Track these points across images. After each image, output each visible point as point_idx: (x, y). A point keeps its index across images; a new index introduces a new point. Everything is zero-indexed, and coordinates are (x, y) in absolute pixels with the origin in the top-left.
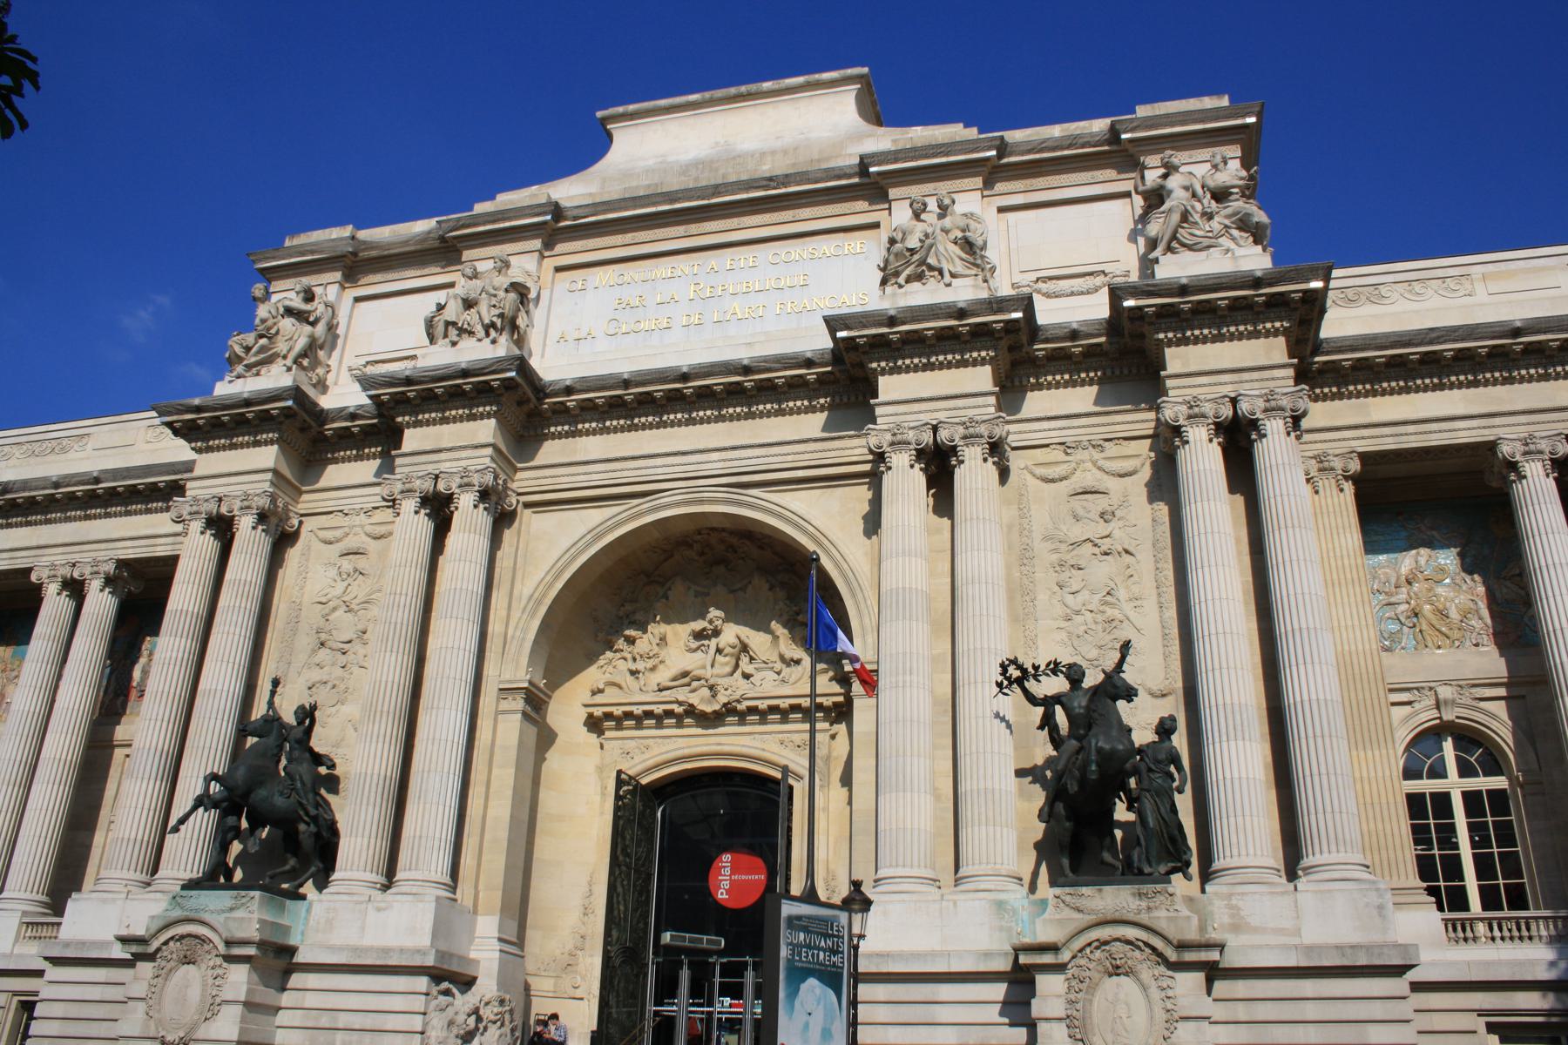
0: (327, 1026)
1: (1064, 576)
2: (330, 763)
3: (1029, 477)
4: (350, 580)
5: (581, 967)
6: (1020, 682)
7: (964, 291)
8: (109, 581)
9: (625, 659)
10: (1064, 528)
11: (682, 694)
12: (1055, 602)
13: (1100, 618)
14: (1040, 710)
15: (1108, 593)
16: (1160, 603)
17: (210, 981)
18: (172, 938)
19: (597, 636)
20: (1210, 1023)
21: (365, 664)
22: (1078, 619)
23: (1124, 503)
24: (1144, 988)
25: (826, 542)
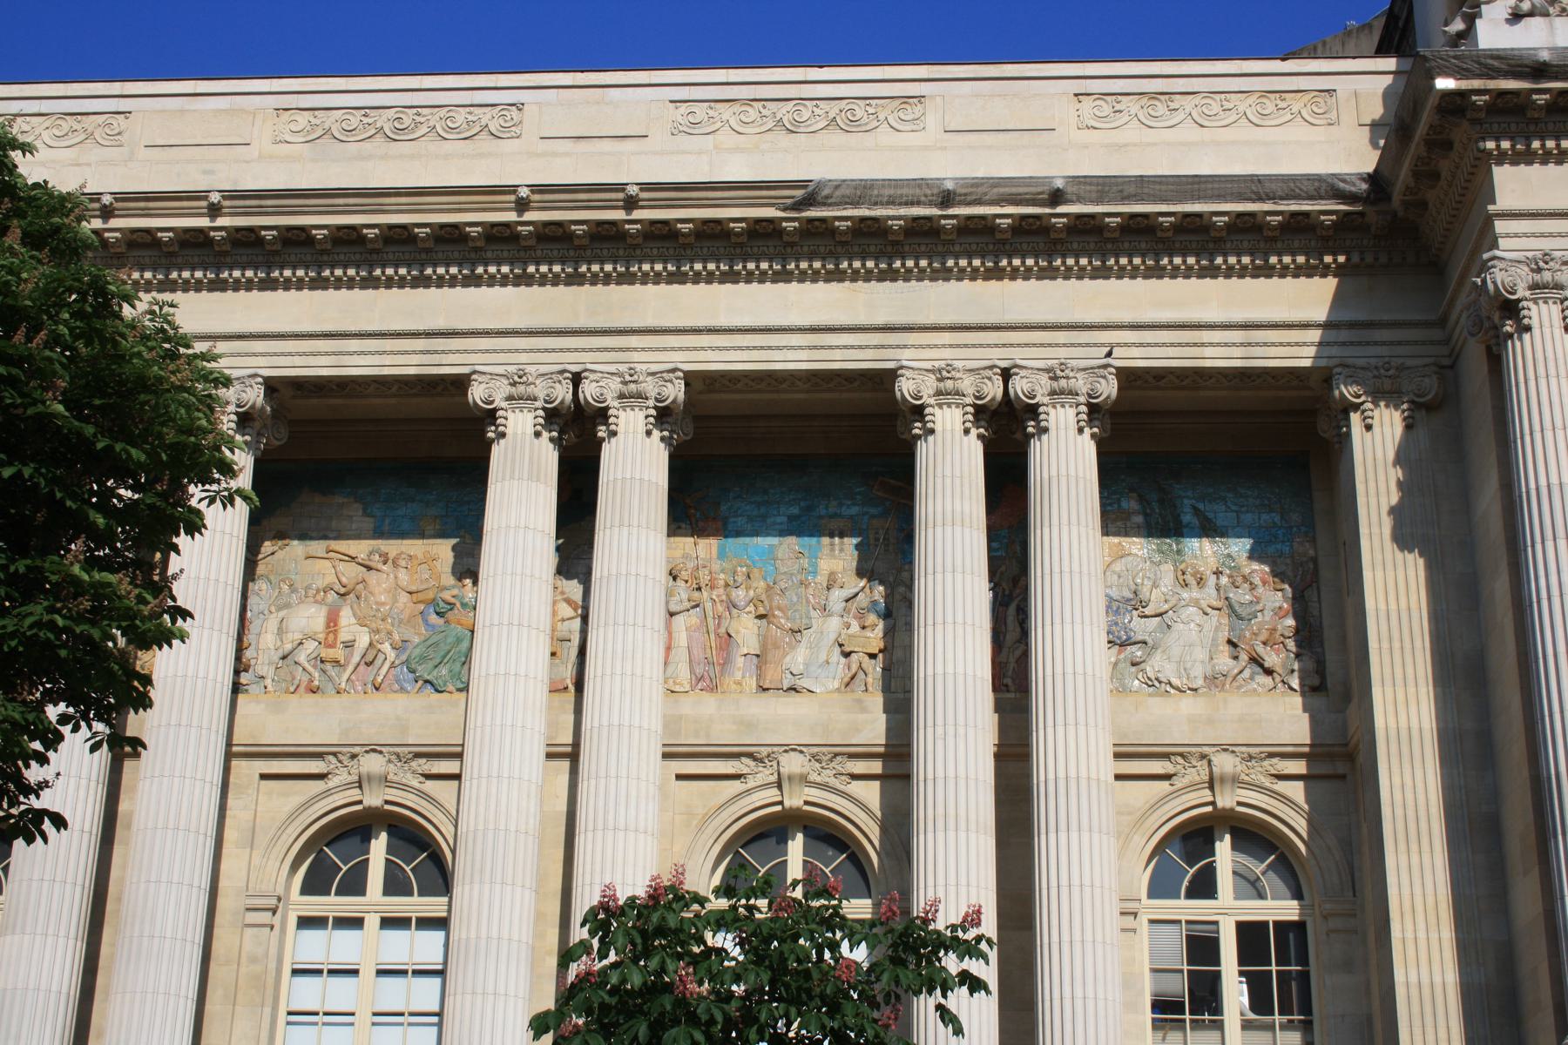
8: (1095, 411)
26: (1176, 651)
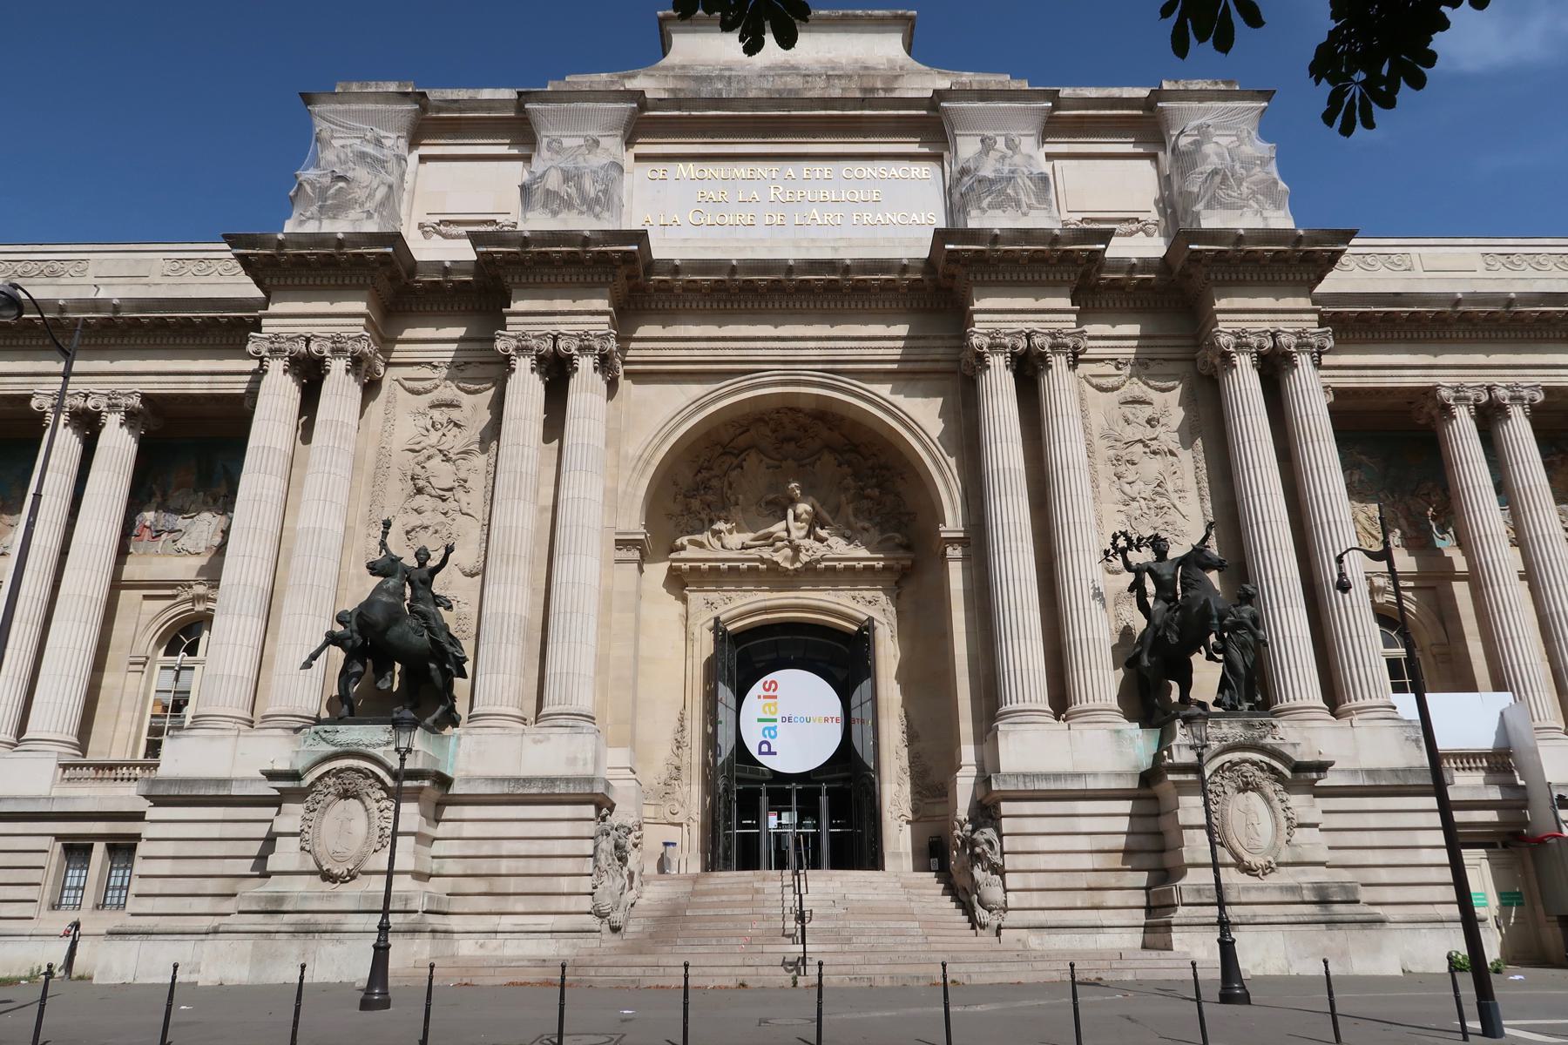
0: (490, 853)
1: (1122, 469)
2: (447, 604)
3: (1086, 385)
4: (445, 431)
5: (678, 795)
6: (1123, 552)
7: (1037, 220)
9: (702, 520)
10: (1118, 429)
11: (766, 553)
12: (1114, 489)
13: (1152, 505)
14: (1131, 577)
15: (1158, 485)
16: (1200, 495)
17: (377, 814)
18: (328, 772)
19: (675, 499)
20: (1321, 830)
21: (469, 511)
22: (1135, 504)
23: (1165, 412)
24: (1267, 800)
25: (915, 427)
26: (194, 535)
